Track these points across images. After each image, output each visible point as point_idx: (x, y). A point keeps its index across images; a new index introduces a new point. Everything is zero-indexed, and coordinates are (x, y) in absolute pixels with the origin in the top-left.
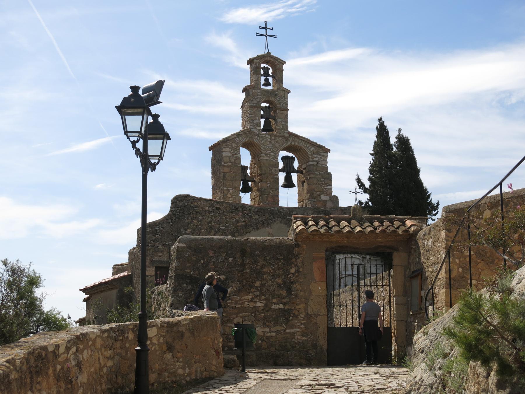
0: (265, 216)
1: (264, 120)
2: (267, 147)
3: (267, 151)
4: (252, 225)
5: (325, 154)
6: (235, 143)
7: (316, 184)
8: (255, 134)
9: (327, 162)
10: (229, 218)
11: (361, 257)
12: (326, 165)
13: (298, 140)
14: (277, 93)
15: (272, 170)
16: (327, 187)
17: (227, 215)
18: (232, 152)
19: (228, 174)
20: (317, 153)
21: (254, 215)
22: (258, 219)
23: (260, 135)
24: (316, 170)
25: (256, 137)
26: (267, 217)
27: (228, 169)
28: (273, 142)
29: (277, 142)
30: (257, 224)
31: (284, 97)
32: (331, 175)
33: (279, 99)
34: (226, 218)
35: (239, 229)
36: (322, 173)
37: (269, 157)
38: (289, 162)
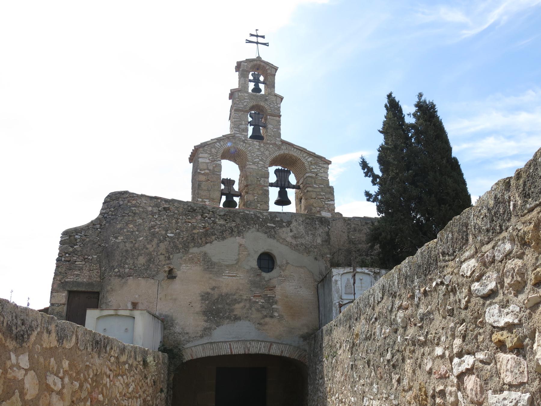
0: (235, 221)
1: (252, 127)
2: (255, 154)
3: (255, 159)
4: (216, 232)
5: (325, 166)
6: (215, 149)
7: (315, 198)
8: (240, 139)
9: (328, 175)
10: (182, 223)
11: (372, 272)
12: (327, 178)
13: (293, 149)
14: (267, 98)
15: (260, 181)
16: (329, 202)
17: (179, 219)
18: (211, 158)
19: (204, 183)
20: (316, 164)
21: (219, 220)
22: (224, 225)
23: (246, 141)
24: (315, 183)
25: (242, 143)
26: (238, 222)
27: (205, 177)
28: (262, 149)
29: (267, 150)
30: (222, 232)
31: (276, 102)
32: (333, 189)
33: (270, 104)
34: (177, 223)
35: (196, 237)
36: (323, 186)
37: (257, 166)
38: (283, 176)
